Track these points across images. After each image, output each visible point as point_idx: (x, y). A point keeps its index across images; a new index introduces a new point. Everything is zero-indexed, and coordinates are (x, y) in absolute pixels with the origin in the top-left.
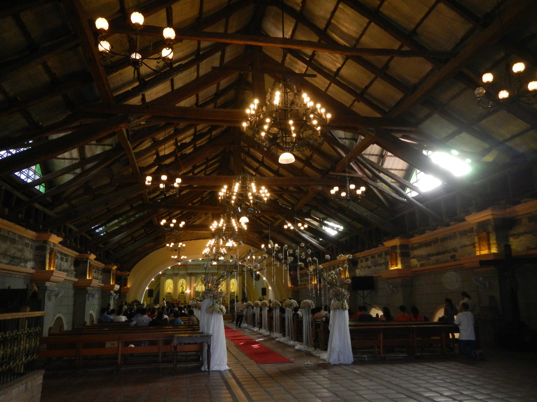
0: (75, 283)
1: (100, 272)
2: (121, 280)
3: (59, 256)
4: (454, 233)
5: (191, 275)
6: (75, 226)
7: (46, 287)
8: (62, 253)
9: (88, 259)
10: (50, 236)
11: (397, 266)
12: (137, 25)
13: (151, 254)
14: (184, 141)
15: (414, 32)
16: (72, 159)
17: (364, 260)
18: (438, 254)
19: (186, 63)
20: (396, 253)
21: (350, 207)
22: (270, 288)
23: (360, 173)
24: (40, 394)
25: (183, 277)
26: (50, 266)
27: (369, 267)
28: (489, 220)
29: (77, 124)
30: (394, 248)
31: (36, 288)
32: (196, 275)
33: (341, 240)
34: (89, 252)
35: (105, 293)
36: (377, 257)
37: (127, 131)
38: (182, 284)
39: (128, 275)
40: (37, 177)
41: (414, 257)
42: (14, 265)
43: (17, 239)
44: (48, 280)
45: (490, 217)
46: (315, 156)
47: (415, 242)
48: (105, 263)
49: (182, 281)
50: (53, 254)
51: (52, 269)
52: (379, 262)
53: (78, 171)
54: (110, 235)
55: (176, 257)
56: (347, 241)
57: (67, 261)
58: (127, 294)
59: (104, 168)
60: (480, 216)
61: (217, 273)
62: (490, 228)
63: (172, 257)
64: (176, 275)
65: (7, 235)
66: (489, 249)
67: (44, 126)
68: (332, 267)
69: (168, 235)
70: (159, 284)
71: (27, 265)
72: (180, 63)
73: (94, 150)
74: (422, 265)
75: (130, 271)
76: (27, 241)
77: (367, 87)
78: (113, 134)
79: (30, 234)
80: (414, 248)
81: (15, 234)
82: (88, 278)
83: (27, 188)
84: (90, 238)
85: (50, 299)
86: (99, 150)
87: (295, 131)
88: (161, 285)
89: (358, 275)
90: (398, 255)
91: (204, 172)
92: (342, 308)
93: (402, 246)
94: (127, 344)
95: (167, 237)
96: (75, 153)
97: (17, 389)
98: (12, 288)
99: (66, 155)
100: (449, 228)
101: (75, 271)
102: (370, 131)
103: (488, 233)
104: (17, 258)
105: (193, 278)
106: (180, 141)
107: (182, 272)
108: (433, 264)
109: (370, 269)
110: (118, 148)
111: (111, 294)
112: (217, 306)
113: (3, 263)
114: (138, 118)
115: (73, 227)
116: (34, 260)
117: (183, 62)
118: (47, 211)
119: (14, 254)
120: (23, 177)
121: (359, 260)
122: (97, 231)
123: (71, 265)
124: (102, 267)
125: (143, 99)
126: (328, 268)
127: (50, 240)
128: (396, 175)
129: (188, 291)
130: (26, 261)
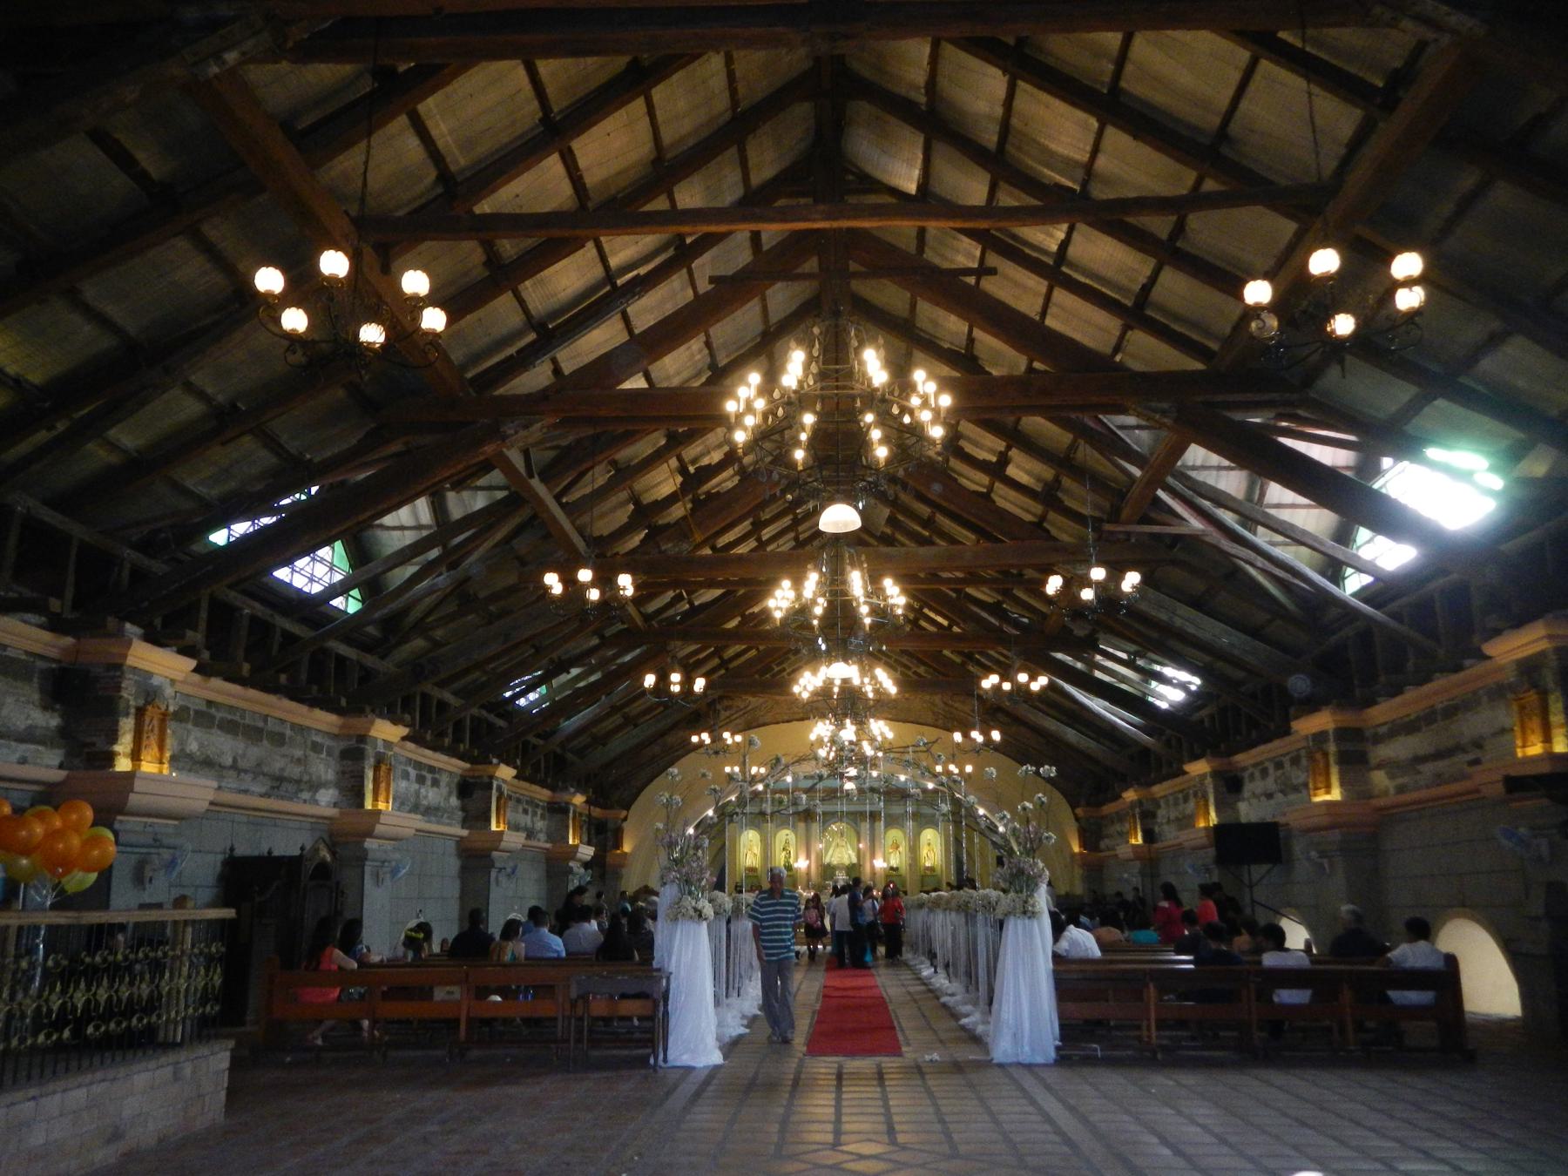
0: (461, 841)
1: (539, 812)
2: (604, 835)
3: (413, 773)
4: (1475, 693)
5: (807, 816)
6: (455, 694)
7: (365, 851)
8: (418, 765)
9: (491, 777)
10: (372, 723)
11: (1328, 792)
12: (333, 279)
14: (705, 461)
15: (1222, 134)
16: (419, 527)
17: (1257, 774)
18: (1438, 755)
19: (650, 272)
20: (1326, 755)
21: (1178, 622)
23: (1196, 524)
24: (223, 1094)
26: (376, 799)
27: (1269, 796)
28: (1542, 654)
29: (396, 447)
30: (1320, 737)
31: (325, 854)
33: (1196, 716)
34: (495, 761)
35: (555, 864)
36: (1287, 765)
37: (526, 454)
38: (787, 842)
39: (625, 819)
40: (338, 577)
41: (1379, 767)
42: (282, 798)
43: (288, 732)
44: (369, 834)
45: (1544, 645)
46: (1067, 482)
47: (1382, 720)
48: (553, 789)
49: (785, 836)
50: (383, 768)
51: (381, 806)
52: (1295, 782)
53: (434, 553)
54: (559, 709)
56: (1212, 717)
57: (435, 783)
58: (624, 871)
59: (496, 546)
60: (1524, 640)
62: (1549, 679)
65: (261, 724)
66: (1547, 739)
67: (317, 459)
69: (726, 709)
71: (318, 796)
72: (634, 273)
73: (466, 503)
74: (1401, 790)
75: (628, 808)
76: (318, 739)
77: (1147, 288)
78: (486, 467)
79: (324, 720)
80: (1378, 740)
81: (283, 721)
82: (494, 827)
83: (311, 608)
84: (501, 723)
85: (378, 881)
86: (479, 502)
87: (882, 441)
89: (1244, 820)
90: (1332, 759)
91: (792, 535)
92: (1025, 913)
93: (1342, 734)
94: (482, 993)
95: (724, 714)
96: (421, 510)
97: (148, 1075)
98: (276, 853)
99: (403, 515)
100: (1461, 675)
101: (463, 809)
102: (1155, 411)
103: (1544, 694)
104: (290, 780)
106: (693, 462)
108: (1428, 787)
109: (1272, 802)
110: (516, 499)
111: (571, 870)
112: (689, 902)
113: (253, 793)
114: (526, 427)
115: (448, 696)
116: (337, 785)
117: (643, 271)
118: (370, 660)
119: (282, 770)
120: (299, 582)
121: (1246, 775)
122: (522, 702)
123: (450, 793)
125: (557, 371)
127: (373, 733)
128: (1292, 526)
129: (801, 864)
130: (315, 786)
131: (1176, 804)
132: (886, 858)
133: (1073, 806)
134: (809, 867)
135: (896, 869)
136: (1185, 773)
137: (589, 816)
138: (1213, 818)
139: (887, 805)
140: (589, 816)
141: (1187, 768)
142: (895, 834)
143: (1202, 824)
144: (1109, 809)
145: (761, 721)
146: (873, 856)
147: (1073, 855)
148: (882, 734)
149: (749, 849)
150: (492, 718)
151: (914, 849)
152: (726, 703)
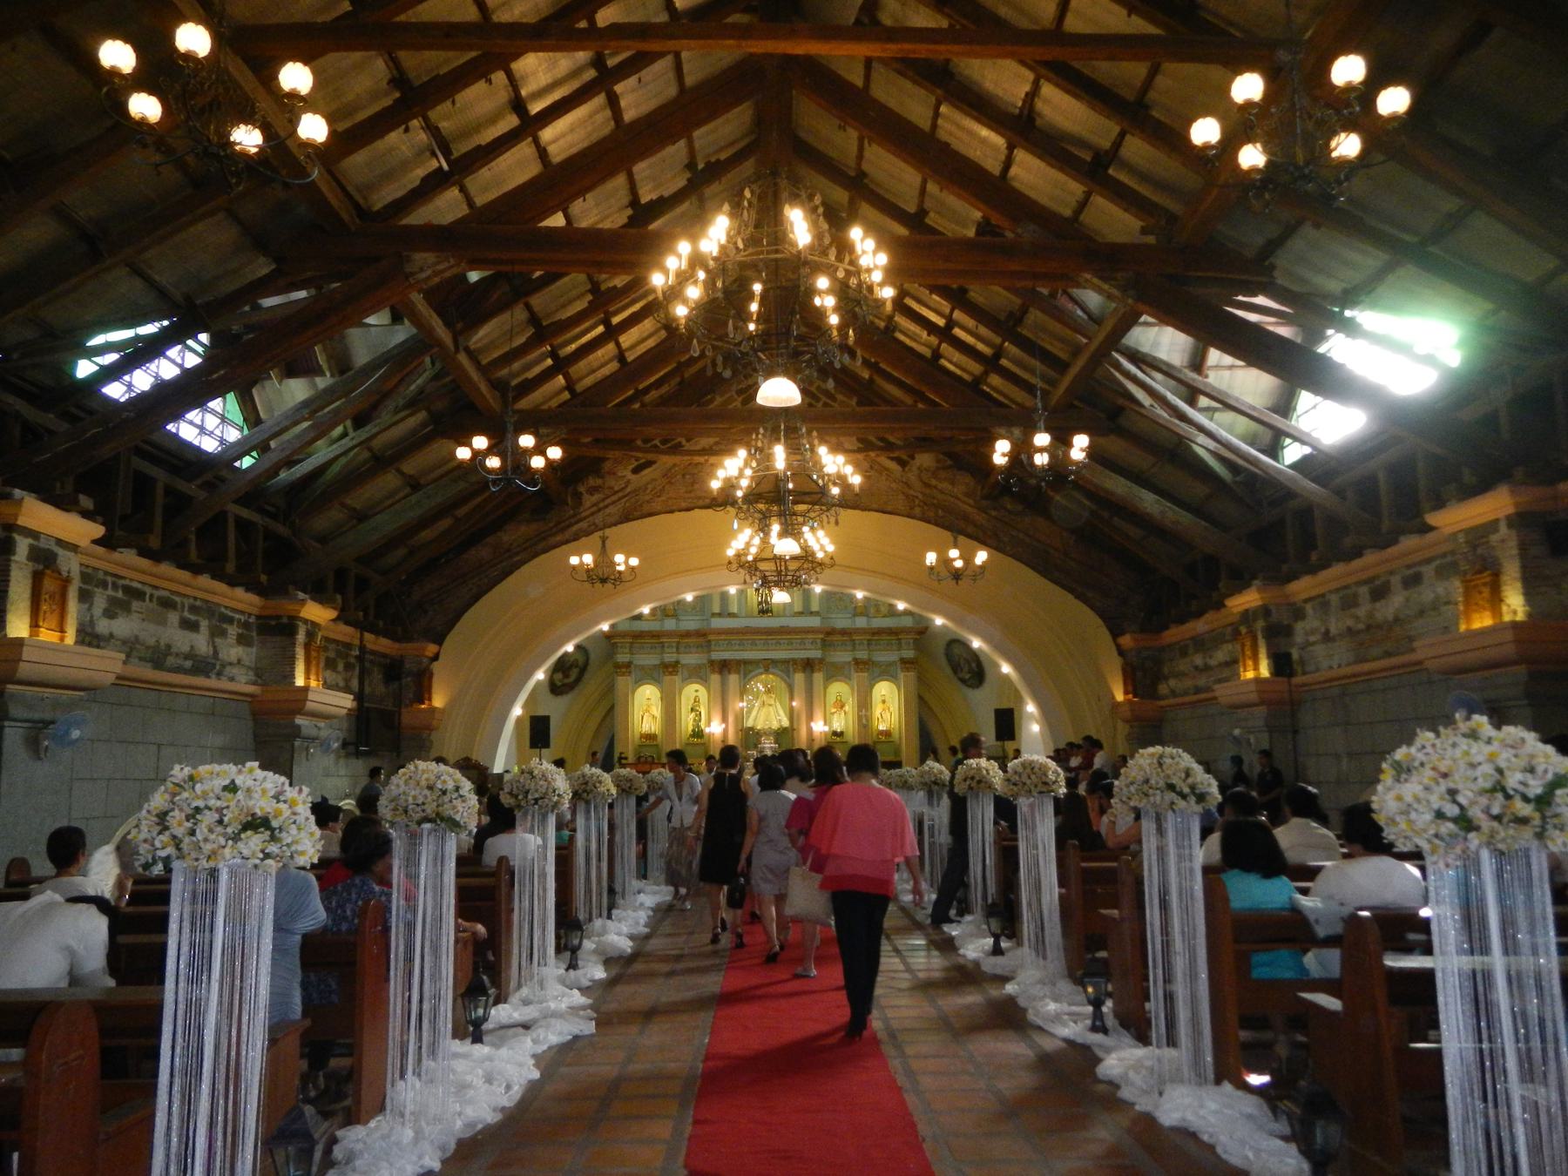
1: (233, 631)
5: (724, 667)
9: (11, 527)
13: (526, 569)
22: (1031, 708)
25: (697, 674)
32: (745, 668)
38: (696, 700)
39: (436, 658)
49: (693, 692)
55: (588, 559)
58: (434, 736)
61: (821, 661)
63: (574, 560)
64: (671, 668)
68: (1364, 591)
69: (593, 490)
70: (612, 708)
75: (439, 641)
88: (618, 709)
95: (589, 500)
105: (733, 679)
107: (690, 659)
124: (255, 611)
126: (1334, 599)
129: (715, 728)
131: (1349, 603)
132: (830, 719)
133: (1116, 633)
134: (725, 731)
135: (841, 734)
136: (1427, 529)
137: (362, 648)
138: (1515, 604)
139: (827, 647)
140: (362, 648)
141: (1433, 519)
142: (838, 689)
143: (1482, 621)
144: (1174, 634)
145: (646, 509)
146: (810, 718)
147: (1116, 705)
148: (841, 480)
149: (645, 709)
150: (49, 419)
151: (864, 704)
152: (593, 481)
